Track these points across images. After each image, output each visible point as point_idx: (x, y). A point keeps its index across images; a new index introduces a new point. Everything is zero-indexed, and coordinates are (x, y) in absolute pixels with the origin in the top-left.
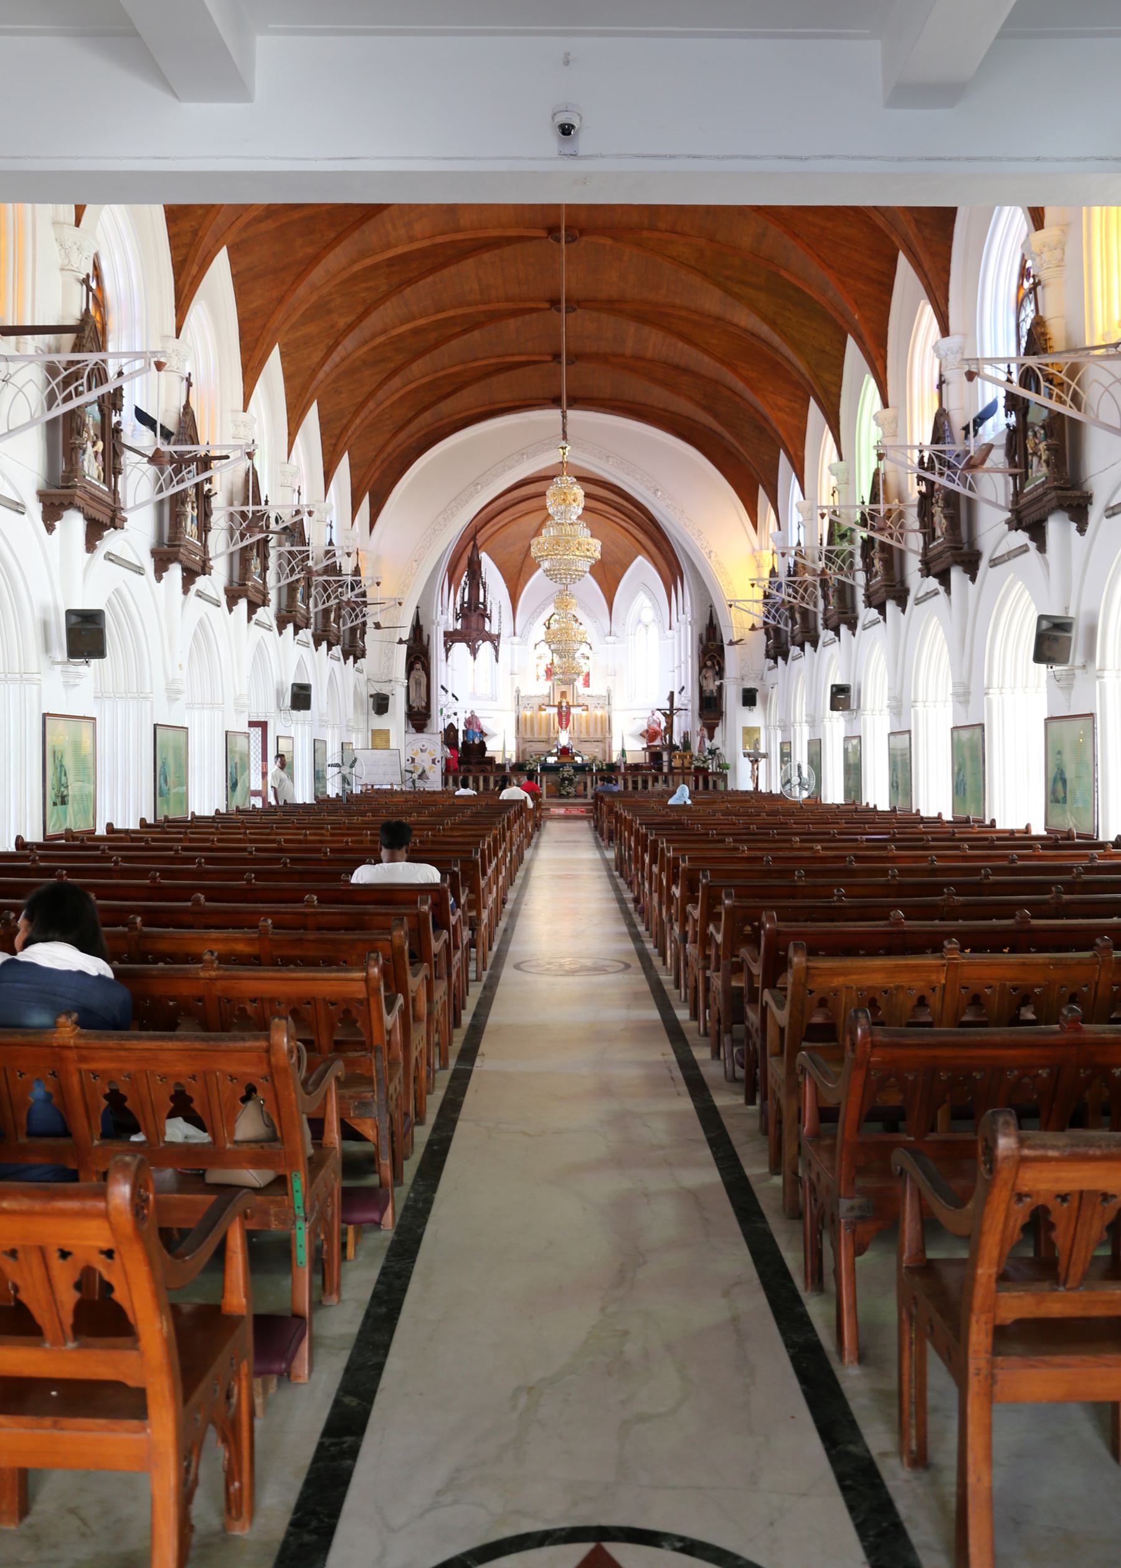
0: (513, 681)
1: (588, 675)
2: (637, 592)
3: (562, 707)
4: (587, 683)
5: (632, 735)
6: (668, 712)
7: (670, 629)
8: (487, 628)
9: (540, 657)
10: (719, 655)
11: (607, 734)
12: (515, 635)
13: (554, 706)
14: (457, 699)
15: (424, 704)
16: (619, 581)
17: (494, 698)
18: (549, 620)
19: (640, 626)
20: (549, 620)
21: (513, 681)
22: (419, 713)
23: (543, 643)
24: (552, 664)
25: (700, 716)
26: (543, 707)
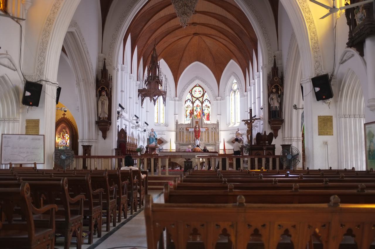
0: (175, 117)
1: (209, 115)
2: (230, 76)
3: (196, 128)
4: (208, 119)
5: (228, 142)
6: (249, 121)
7: (246, 92)
8: (160, 88)
9: (187, 107)
10: (281, 85)
11: (217, 142)
12: (176, 97)
13: (193, 128)
14: (147, 124)
15: (106, 116)
16: (222, 72)
17: (166, 125)
18: (192, 90)
19: (232, 92)
20: (192, 90)
21: (175, 117)
22: (103, 121)
23: (189, 101)
24: (193, 110)
25: (269, 122)
26: (188, 129)
